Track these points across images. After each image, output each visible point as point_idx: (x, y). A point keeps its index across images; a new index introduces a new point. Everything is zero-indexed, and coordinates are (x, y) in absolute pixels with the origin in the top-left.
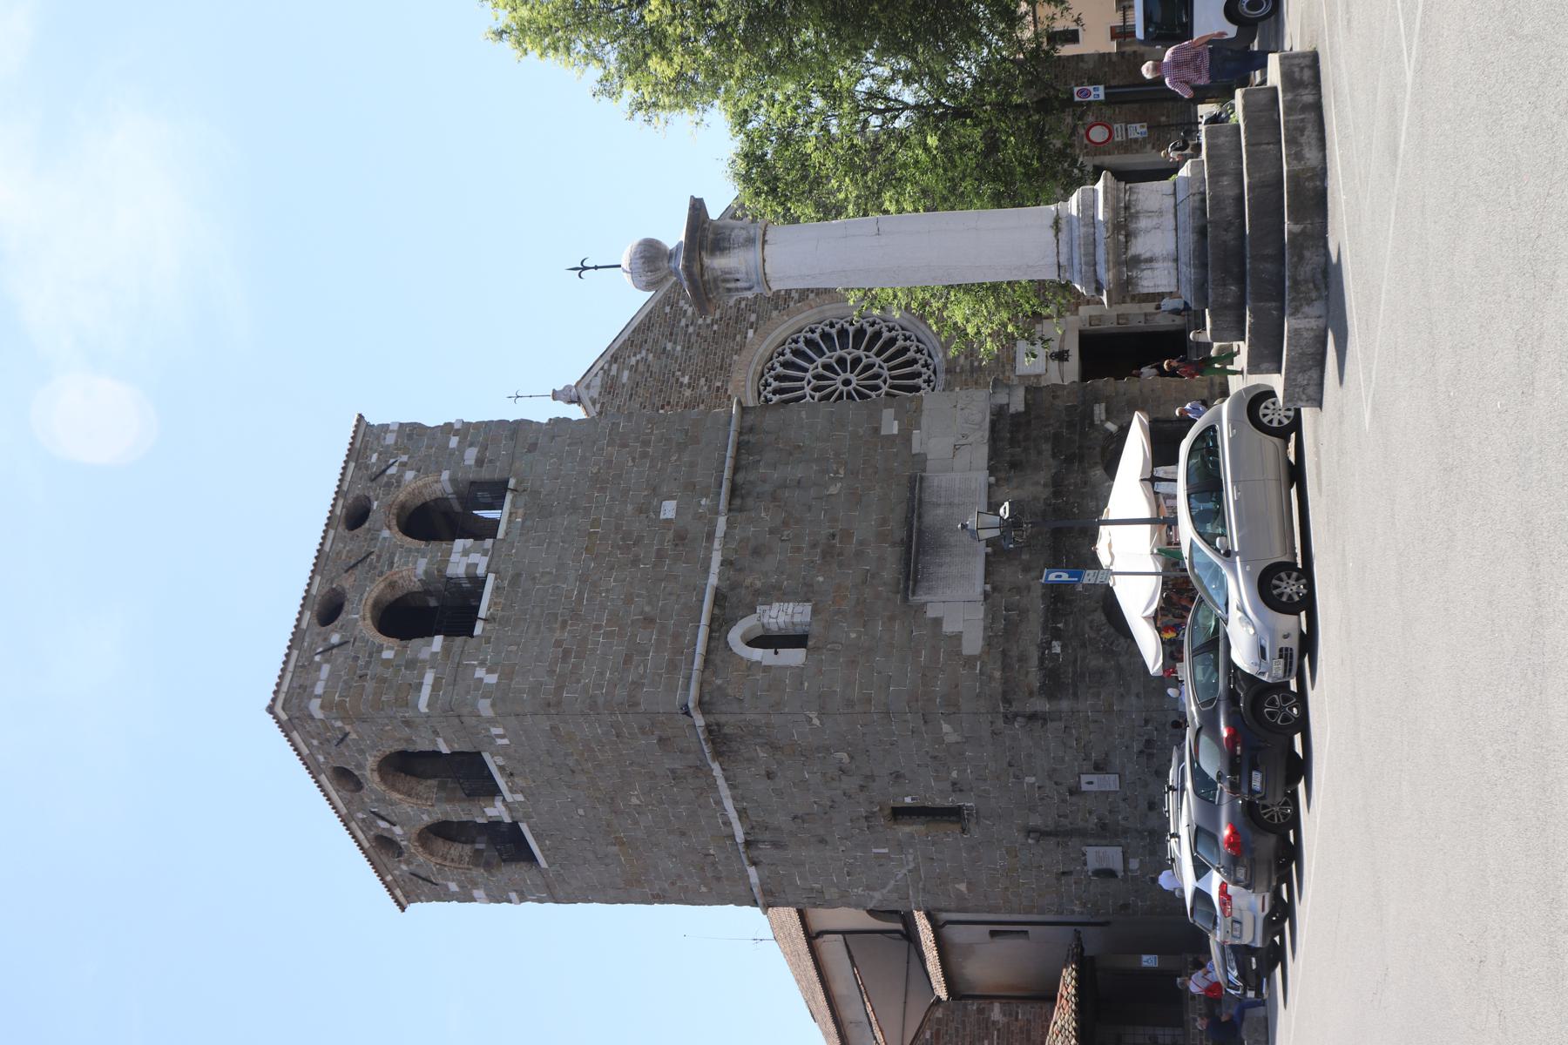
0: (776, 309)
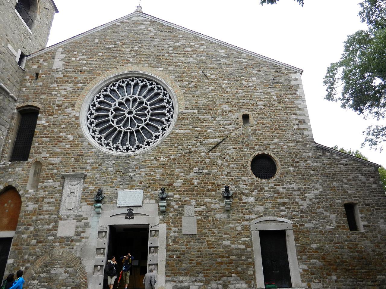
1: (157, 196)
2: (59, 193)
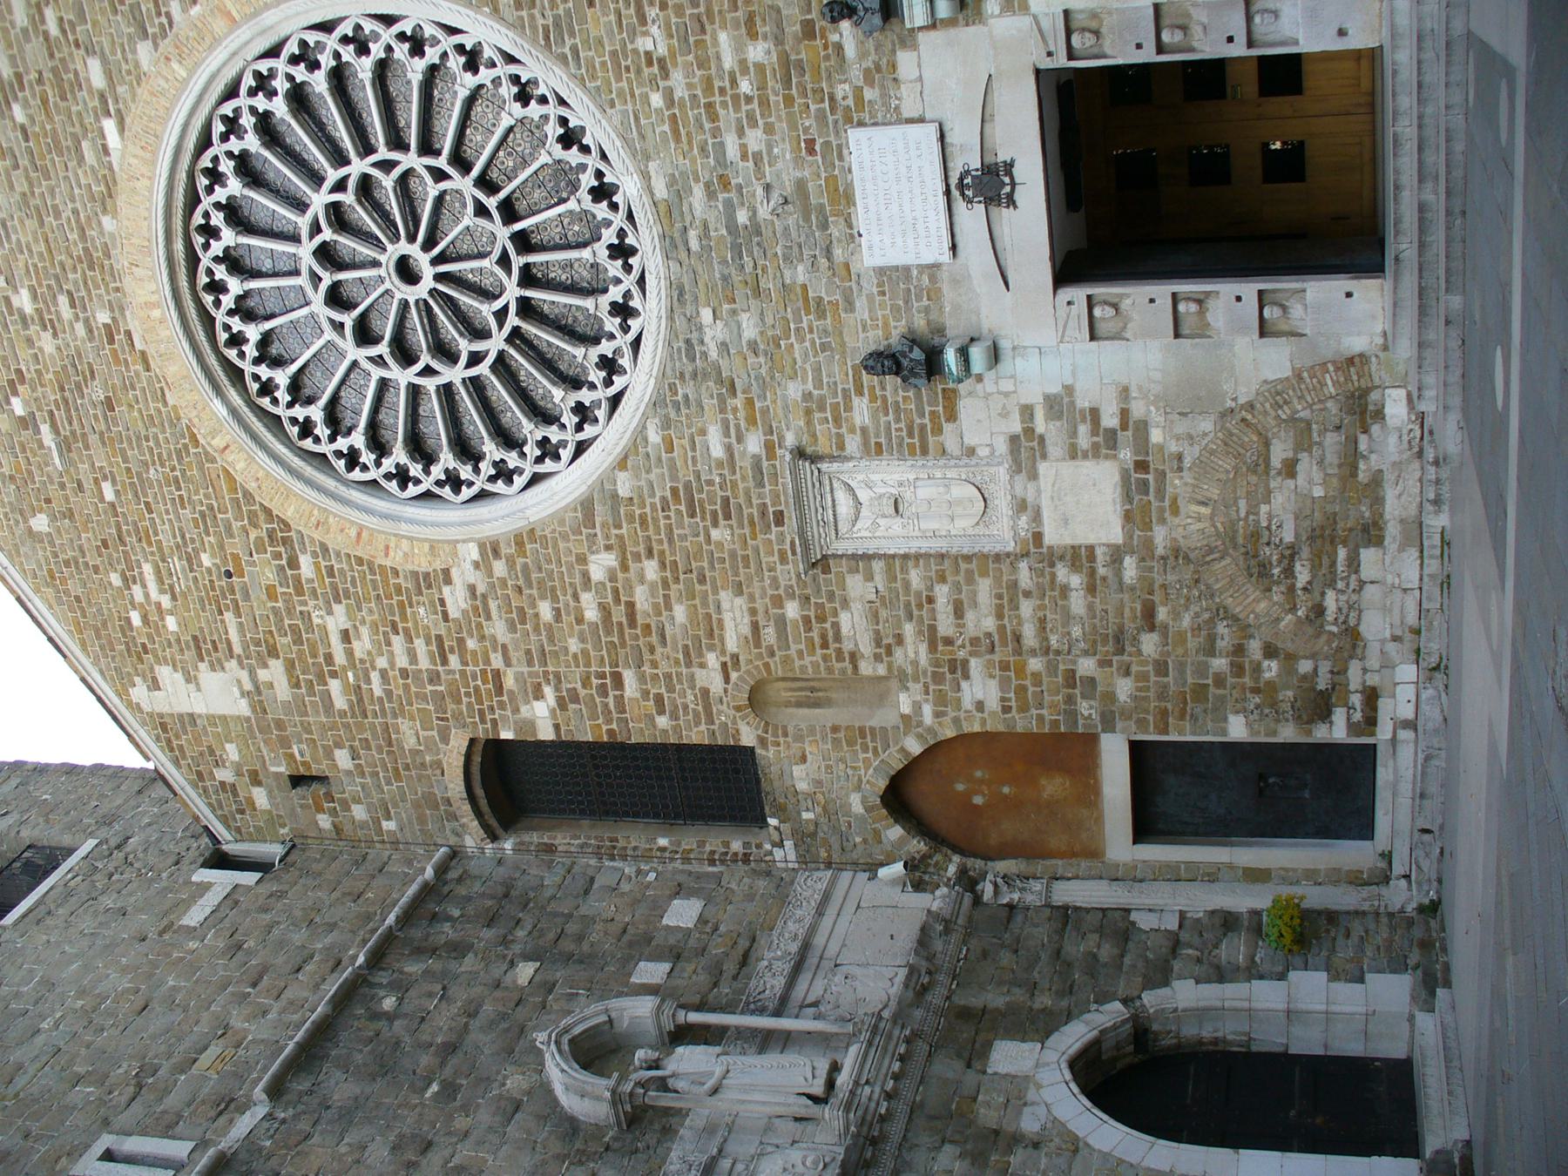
0: (145, 35)
1: (870, 45)
2: (904, 570)
